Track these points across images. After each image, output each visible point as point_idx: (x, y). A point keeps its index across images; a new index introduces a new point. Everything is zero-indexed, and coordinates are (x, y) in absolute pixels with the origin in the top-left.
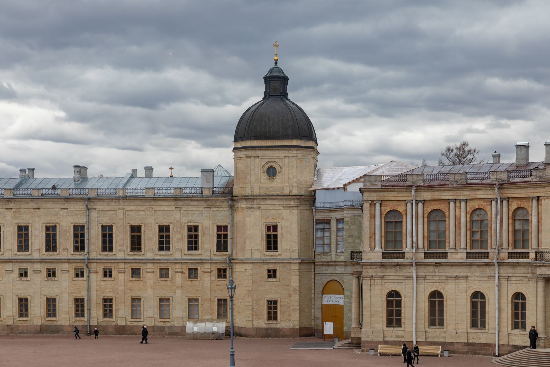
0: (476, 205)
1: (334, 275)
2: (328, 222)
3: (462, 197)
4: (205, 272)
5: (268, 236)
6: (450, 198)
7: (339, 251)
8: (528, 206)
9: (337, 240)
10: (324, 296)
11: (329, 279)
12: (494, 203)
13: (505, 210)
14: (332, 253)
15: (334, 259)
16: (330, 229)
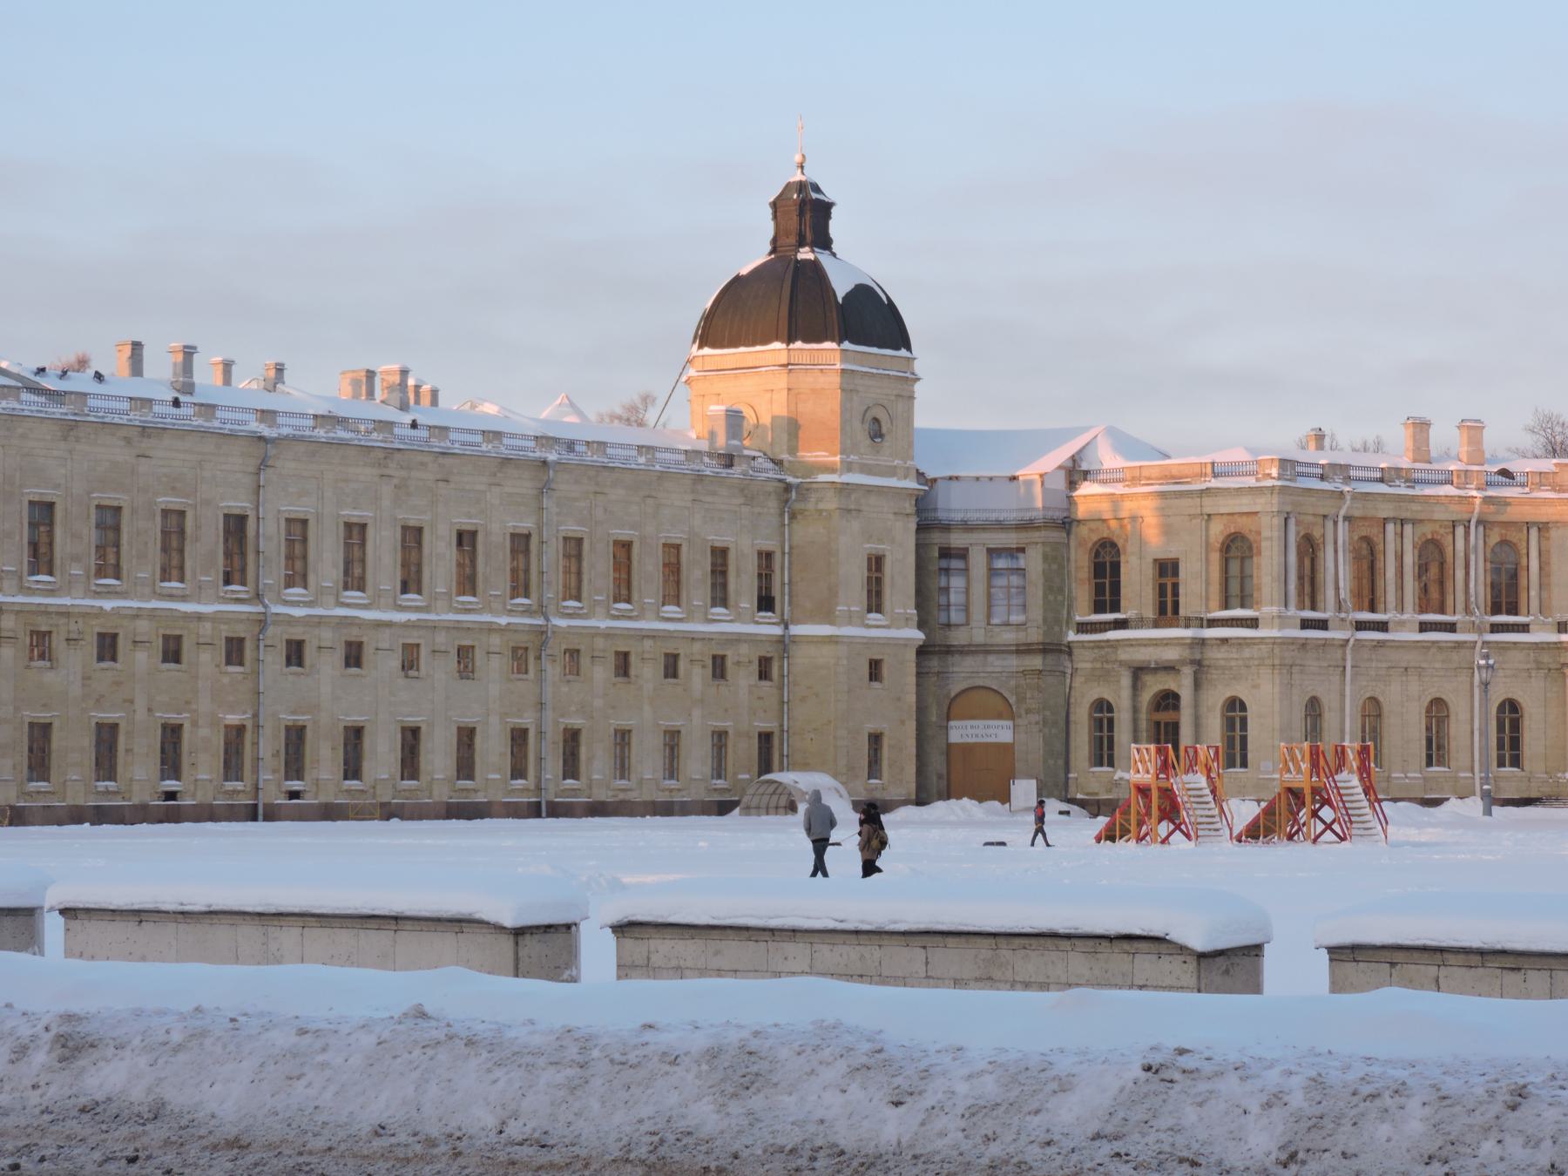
0: (1427, 530)
1: (982, 675)
2: (963, 554)
3: (1407, 515)
4: (738, 663)
5: (869, 578)
6: (1391, 514)
7: (995, 621)
8: (1520, 540)
9: (989, 596)
10: (952, 723)
11: (965, 685)
12: (1460, 531)
13: (1481, 543)
14: (973, 624)
15: (979, 636)
16: (967, 570)
